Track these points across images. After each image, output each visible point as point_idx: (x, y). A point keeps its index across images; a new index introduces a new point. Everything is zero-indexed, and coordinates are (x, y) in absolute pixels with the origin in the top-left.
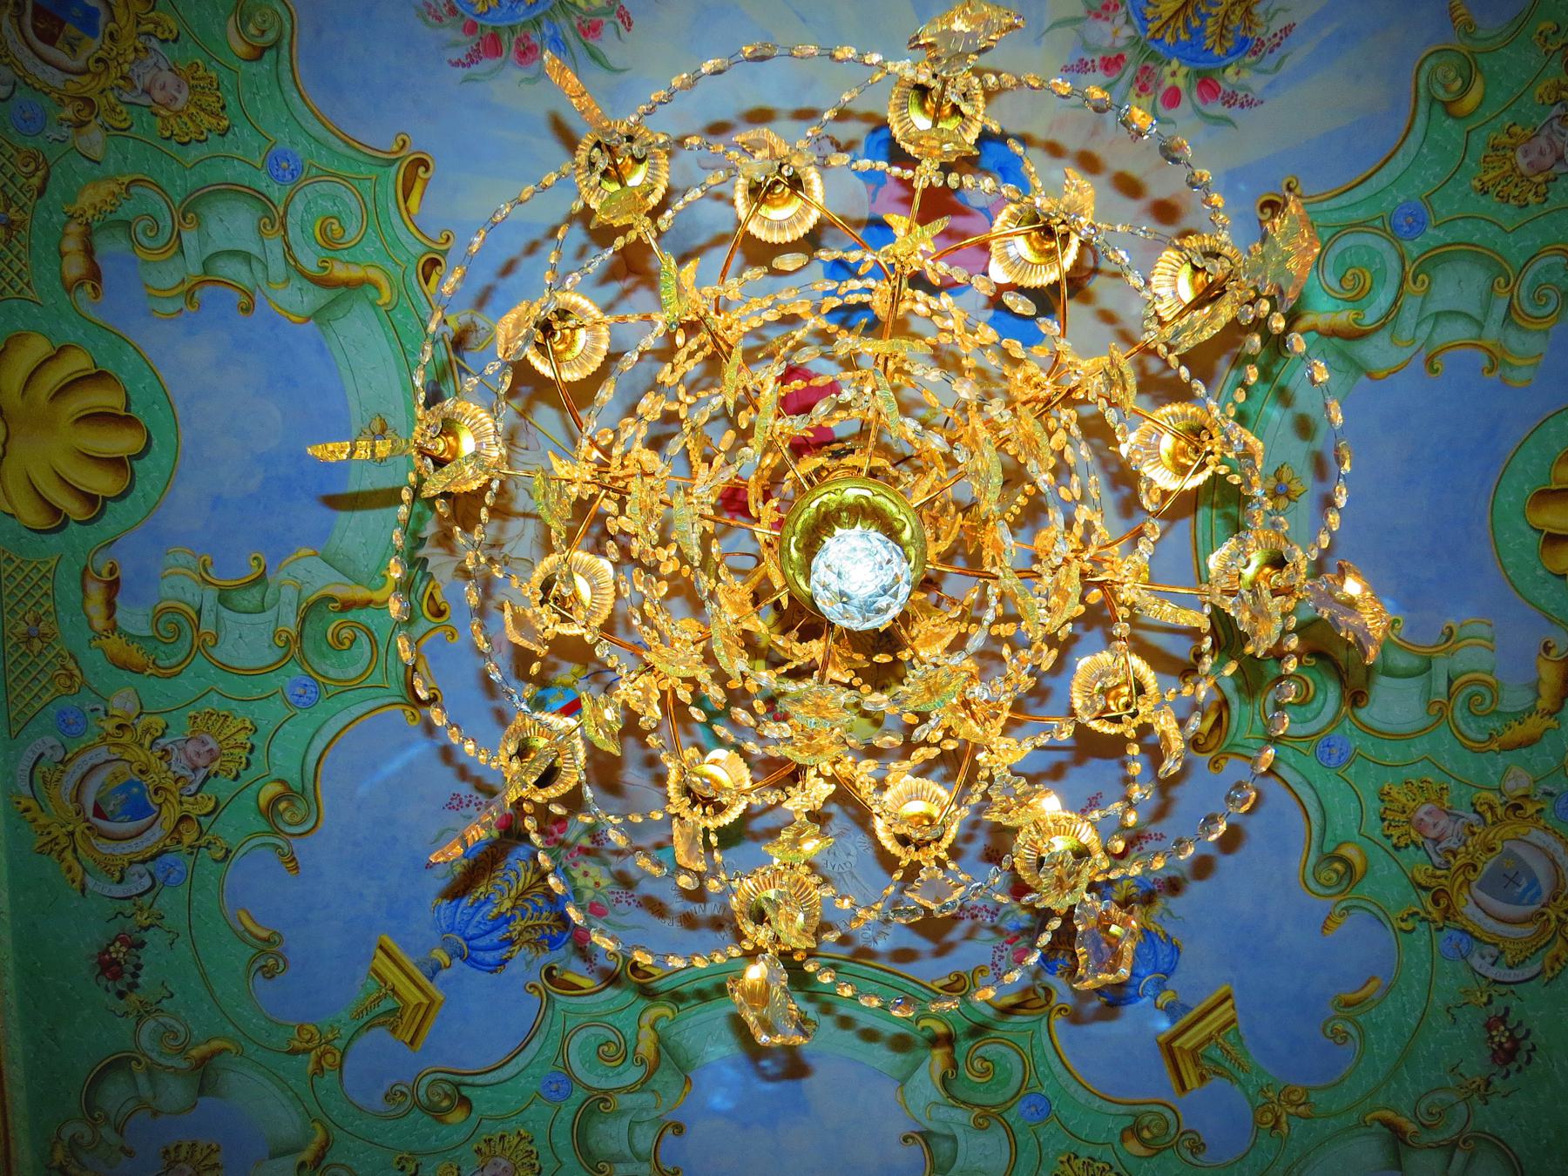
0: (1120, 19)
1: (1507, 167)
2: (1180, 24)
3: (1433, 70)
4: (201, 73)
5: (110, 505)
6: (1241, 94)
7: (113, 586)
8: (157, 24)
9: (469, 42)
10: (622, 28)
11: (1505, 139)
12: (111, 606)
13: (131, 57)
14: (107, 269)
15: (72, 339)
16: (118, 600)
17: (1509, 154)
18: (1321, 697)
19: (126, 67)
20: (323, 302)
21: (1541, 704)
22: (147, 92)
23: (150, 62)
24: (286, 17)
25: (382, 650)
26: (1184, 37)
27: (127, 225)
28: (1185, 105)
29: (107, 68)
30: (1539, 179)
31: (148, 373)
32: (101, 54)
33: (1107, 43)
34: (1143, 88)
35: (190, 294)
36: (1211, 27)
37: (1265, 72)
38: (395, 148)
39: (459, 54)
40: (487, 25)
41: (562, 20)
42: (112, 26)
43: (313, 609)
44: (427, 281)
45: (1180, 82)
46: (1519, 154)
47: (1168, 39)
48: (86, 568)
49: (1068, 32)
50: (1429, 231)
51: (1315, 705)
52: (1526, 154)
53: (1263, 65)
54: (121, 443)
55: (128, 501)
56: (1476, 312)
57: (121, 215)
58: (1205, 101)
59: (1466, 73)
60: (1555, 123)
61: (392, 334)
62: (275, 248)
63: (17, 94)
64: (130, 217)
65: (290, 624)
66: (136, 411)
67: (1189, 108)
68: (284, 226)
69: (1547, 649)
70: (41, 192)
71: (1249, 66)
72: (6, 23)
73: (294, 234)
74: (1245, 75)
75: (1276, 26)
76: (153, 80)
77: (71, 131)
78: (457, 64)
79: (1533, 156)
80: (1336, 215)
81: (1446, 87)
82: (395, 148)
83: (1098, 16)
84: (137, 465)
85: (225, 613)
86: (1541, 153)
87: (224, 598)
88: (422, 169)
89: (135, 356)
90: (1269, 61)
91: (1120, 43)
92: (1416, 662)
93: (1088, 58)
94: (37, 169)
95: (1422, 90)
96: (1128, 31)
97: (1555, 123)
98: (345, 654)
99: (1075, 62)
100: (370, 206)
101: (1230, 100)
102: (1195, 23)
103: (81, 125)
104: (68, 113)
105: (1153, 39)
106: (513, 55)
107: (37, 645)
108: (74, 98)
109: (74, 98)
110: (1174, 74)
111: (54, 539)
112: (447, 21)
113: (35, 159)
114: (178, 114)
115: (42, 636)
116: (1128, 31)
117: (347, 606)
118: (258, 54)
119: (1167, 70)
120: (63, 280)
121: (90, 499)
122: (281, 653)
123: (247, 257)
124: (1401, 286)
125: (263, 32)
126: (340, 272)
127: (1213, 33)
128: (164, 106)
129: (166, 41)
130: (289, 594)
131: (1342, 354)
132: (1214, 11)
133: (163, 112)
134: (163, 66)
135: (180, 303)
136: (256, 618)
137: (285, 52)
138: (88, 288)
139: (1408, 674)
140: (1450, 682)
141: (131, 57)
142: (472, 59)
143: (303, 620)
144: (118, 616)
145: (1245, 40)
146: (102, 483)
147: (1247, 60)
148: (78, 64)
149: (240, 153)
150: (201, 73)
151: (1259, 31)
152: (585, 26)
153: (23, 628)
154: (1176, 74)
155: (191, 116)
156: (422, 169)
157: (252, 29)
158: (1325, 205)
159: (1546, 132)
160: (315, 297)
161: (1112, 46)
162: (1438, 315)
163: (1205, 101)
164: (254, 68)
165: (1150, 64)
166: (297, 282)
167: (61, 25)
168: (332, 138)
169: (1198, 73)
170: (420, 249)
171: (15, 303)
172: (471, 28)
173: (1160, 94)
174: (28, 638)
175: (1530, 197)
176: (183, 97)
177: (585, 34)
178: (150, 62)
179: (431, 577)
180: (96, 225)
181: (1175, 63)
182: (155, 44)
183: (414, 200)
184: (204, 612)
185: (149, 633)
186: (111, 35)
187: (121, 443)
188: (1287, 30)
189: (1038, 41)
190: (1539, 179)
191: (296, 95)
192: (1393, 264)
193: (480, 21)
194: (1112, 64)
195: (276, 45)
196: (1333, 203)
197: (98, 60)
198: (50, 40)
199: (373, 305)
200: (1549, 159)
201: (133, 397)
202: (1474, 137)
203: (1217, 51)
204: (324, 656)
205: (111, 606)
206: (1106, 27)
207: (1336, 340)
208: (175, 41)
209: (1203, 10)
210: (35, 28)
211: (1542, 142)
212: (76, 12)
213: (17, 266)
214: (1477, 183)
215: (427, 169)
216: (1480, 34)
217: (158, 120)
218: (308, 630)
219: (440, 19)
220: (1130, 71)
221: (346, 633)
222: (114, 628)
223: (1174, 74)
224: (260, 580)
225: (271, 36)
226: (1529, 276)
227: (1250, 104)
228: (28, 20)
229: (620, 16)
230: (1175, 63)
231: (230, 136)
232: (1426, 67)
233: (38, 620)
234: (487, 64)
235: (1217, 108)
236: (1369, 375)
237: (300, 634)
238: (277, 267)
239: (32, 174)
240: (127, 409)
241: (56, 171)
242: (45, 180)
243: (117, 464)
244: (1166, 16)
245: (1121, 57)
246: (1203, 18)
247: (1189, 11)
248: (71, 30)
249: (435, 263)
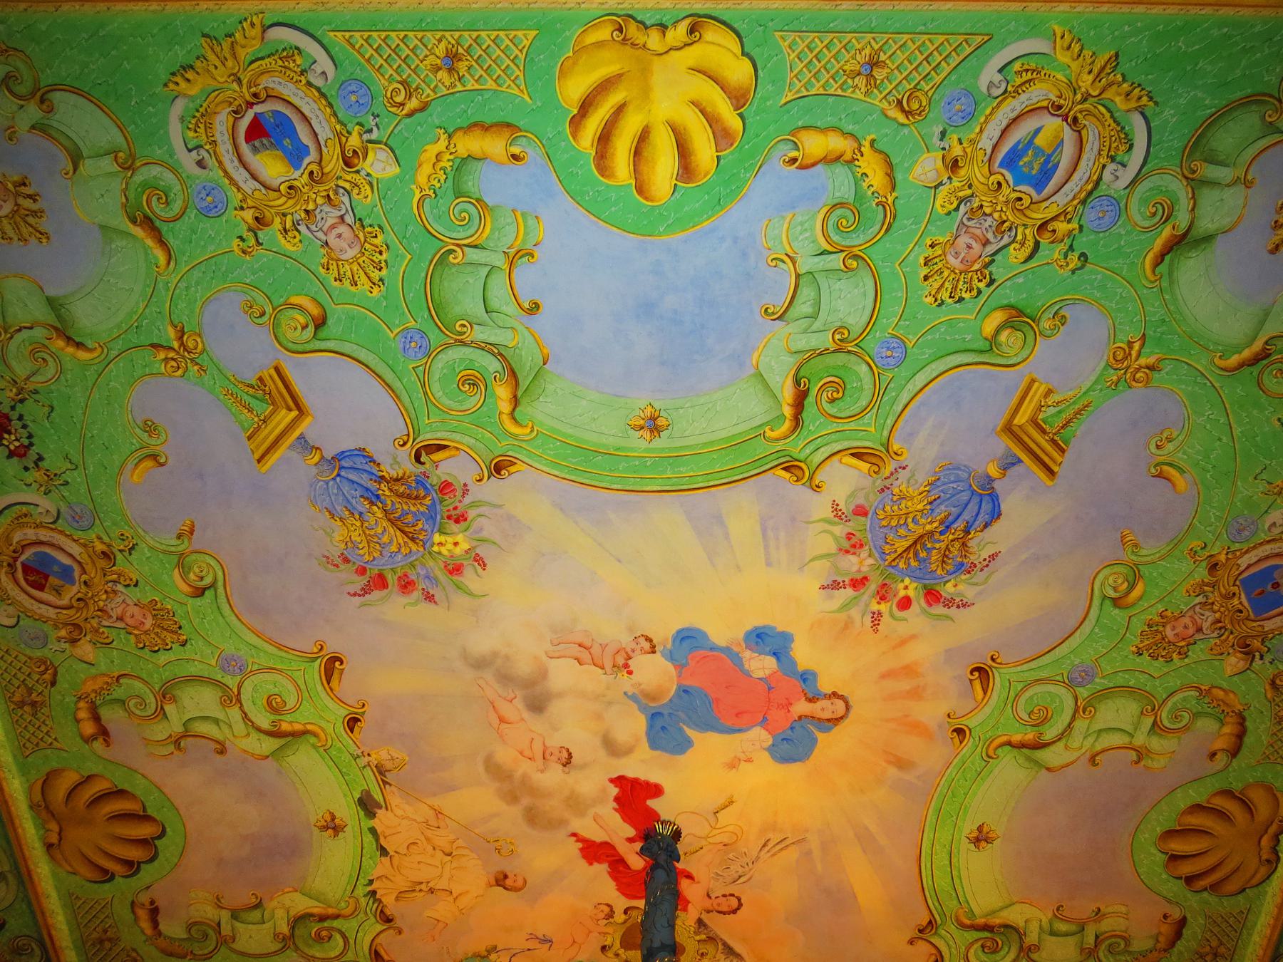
0: (864, 553)
1: (1159, 636)
2: (911, 555)
3: (1106, 578)
4: (159, 606)
5: (143, 866)
6: (958, 600)
7: (154, 912)
8: (119, 575)
9: (361, 581)
10: (479, 568)
11: (1157, 619)
12: (155, 924)
13: (104, 597)
14: (111, 727)
15: (95, 771)
16: (160, 918)
17: (1161, 629)
18: (1006, 949)
19: (101, 603)
20: (277, 746)
21: (1159, 946)
22: (120, 619)
23: (119, 600)
24: (217, 568)
25: (352, 942)
26: (913, 563)
27: (122, 702)
28: (915, 607)
29: (86, 605)
30: (1183, 643)
31: (154, 789)
32: (80, 595)
33: (855, 569)
34: (883, 598)
35: (177, 743)
36: (935, 556)
37: (976, 584)
38: (315, 650)
39: (357, 587)
40: (373, 570)
41: (431, 563)
42: (84, 577)
43: (298, 921)
44: (352, 731)
45: (911, 593)
46: (1168, 628)
47: (902, 565)
48: (133, 902)
49: (826, 563)
50: (1097, 680)
51: (1002, 953)
52: (1174, 628)
53: (974, 580)
54: (145, 831)
55: (156, 863)
56: (1129, 728)
57: (115, 695)
58: (930, 605)
59: (1131, 579)
60: (1197, 609)
61: (331, 763)
62: (235, 713)
63: (21, 623)
64: (124, 698)
65: (285, 929)
66: (150, 812)
67: (918, 610)
68: (239, 701)
69: (1165, 917)
70: (53, 684)
71: (964, 581)
72: (4, 578)
73: (247, 706)
74: (961, 587)
75: (985, 554)
76: (124, 612)
77: (67, 645)
78: (355, 595)
79: (1179, 629)
80: (1026, 674)
81: (1115, 589)
82: (315, 650)
83: (847, 552)
84: (157, 842)
85: (238, 925)
86: (1185, 627)
87: (235, 915)
88: (337, 663)
89: (144, 781)
90: (979, 576)
91: (865, 569)
92: (1073, 928)
93: (840, 579)
94: (47, 669)
95: (1096, 591)
96: (870, 561)
97: (1197, 609)
98: (326, 945)
99: (830, 582)
100: (303, 687)
101: (949, 603)
102: (923, 555)
103: (74, 641)
104: (63, 633)
105: (890, 566)
106: (396, 589)
107: (107, 945)
108: (66, 624)
109: (66, 624)
110: (906, 588)
111: (107, 886)
112: (342, 567)
113: (45, 663)
114: (146, 633)
115: (110, 940)
116: (870, 561)
117: (323, 918)
118: (200, 592)
119: (901, 586)
120: (82, 737)
121: (129, 864)
122: (281, 946)
123: (216, 721)
124: (1074, 715)
125: (202, 578)
126: (285, 727)
127: (937, 560)
128: (135, 628)
129: (128, 586)
130: (280, 913)
131: (1028, 759)
132: (937, 546)
133: (136, 632)
134: (129, 601)
135: (172, 748)
136: (260, 927)
137: (221, 590)
138: (101, 740)
139: (1066, 935)
140: (1097, 937)
141: (104, 597)
142: (366, 591)
143: (293, 928)
144: (161, 927)
145: (962, 564)
146: (134, 853)
147: (963, 577)
148: (65, 602)
149: (198, 657)
150: (159, 606)
151: (973, 558)
152: (450, 567)
153: (95, 935)
154: (909, 587)
155: (157, 634)
156: (337, 663)
157: (192, 576)
158: (1019, 669)
159: (1190, 613)
160: (269, 745)
161: (859, 571)
162: (1100, 731)
163: (930, 605)
164: (198, 601)
165: (887, 581)
166: (255, 735)
167: (46, 577)
168: (266, 645)
169: (925, 586)
170: (343, 712)
171: (49, 751)
172: (362, 571)
173: (896, 600)
174: (101, 941)
175: (1175, 655)
176: (149, 623)
177: (451, 573)
178: (119, 600)
179: (380, 901)
180: (98, 702)
181: (907, 581)
182: (120, 587)
183: (334, 683)
184: (223, 925)
185: (185, 936)
186: (85, 583)
187: (145, 831)
188: (993, 557)
189: (801, 568)
190: (1183, 643)
191: (234, 618)
192: (1069, 702)
193: (368, 566)
194: (858, 583)
195: (213, 585)
196: (1025, 667)
197: (79, 600)
198: (41, 588)
199: (314, 746)
200: (1191, 631)
201: (147, 804)
202: (1134, 620)
203: (939, 572)
204: (310, 946)
205: (155, 924)
206: (853, 558)
207: (1025, 751)
208: (136, 585)
209: (929, 546)
210: (26, 580)
211: (1187, 620)
212: (56, 568)
213: (44, 729)
214: (1134, 649)
215: (342, 663)
216: (1144, 552)
217: (132, 637)
218: (297, 932)
219: (337, 566)
220: (872, 587)
221: (324, 933)
222: (160, 934)
223: (906, 588)
224: (258, 906)
225: (208, 580)
226: (1170, 704)
227: (964, 606)
228: (20, 575)
229: (476, 560)
230: (907, 581)
231: (188, 646)
232: (1101, 576)
233: (105, 931)
234: (377, 594)
235: (939, 609)
236: (1048, 769)
237: (293, 935)
238: (240, 727)
239: (44, 672)
240: (145, 810)
241: (61, 671)
242: (55, 674)
243: (143, 842)
244: (900, 550)
245: (866, 578)
246: (929, 551)
247: (918, 547)
248: (53, 580)
249: (356, 720)
